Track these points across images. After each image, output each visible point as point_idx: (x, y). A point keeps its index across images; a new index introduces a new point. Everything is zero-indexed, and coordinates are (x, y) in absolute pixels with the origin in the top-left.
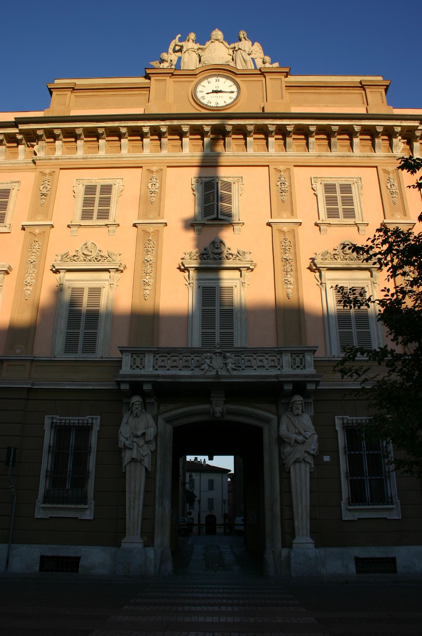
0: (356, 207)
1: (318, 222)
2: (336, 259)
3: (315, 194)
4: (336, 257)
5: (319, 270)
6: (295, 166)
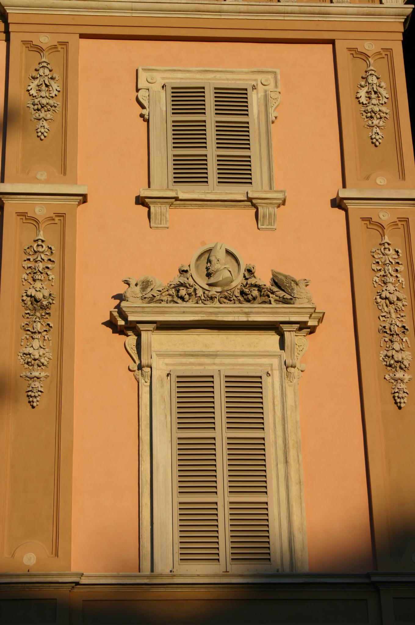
0: (256, 152)
1: (142, 195)
2: (182, 298)
3: (142, 116)
4: (183, 292)
5: (133, 328)
6: (83, 36)
